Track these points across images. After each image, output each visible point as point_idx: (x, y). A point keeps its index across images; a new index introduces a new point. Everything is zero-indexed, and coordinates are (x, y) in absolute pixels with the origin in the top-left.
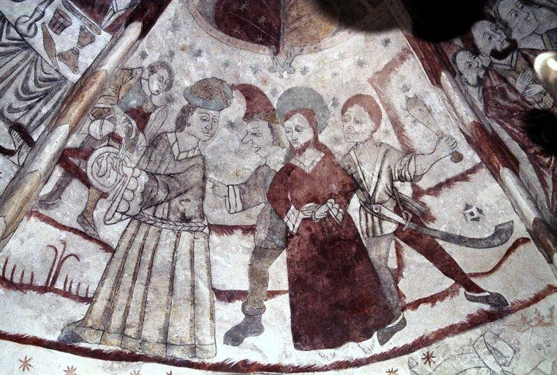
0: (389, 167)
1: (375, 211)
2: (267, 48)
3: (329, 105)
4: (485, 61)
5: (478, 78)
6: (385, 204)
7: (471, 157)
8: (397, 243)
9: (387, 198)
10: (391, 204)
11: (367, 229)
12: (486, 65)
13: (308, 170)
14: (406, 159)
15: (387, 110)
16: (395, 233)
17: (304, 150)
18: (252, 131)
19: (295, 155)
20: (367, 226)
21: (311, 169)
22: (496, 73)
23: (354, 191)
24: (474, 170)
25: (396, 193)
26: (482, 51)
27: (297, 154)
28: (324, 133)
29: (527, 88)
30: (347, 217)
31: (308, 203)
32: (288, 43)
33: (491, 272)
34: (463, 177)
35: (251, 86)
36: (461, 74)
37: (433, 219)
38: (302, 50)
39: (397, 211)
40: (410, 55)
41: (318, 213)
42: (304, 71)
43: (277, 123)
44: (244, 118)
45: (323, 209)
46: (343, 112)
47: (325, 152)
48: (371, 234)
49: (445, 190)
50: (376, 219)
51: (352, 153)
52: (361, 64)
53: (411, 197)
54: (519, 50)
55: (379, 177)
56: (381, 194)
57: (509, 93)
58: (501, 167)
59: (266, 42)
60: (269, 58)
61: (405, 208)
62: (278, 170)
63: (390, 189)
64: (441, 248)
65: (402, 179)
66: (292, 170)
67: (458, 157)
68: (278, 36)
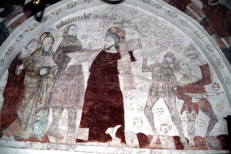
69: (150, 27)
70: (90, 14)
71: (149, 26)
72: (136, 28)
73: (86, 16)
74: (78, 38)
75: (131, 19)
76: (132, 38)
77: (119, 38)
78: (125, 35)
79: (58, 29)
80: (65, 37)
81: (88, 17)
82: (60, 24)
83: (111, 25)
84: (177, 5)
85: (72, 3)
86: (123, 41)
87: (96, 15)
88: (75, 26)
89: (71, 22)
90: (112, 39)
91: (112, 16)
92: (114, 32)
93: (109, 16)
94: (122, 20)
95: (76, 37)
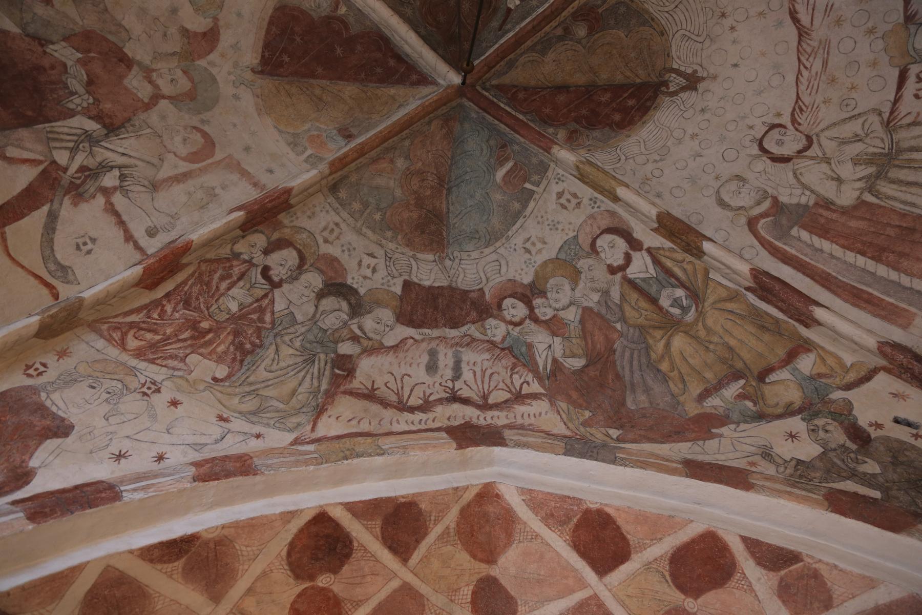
0: (136, 166)
1: (81, 145)
2: (258, 61)
3: (202, 116)
4: (259, 259)
5: (241, 253)
6: (90, 156)
7: (153, 246)
8: (40, 162)
9: (99, 159)
10: (91, 163)
11: (58, 133)
12: (254, 261)
13: (126, 82)
14: (146, 183)
15: (200, 169)
16: (54, 162)
17: (150, 82)
18: (169, 33)
19: (144, 72)
20: (63, 133)
21: (129, 86)
22: (249, 269)
23: (104, 126)
24: (138, 247)
25: (104, 170)
26: (268, 257)
27: (145, 75)
28: (171, 106)
29: (233, 298)
30: (72, 114)
31: (88, 75)
32: (267, 83)
33: (9, 255)
34: (129, 237)
35: (218, 40)
36: (243, 237)
37: (75, 204)
38: (258, 97)
39: (82, 169)
40: (259, 191)
41: (74, 81)
42: (236, 97)
43: (179, 62)
44: (183, 27)
45: (81, 90)
46: (195, 128)
47: (148, 104)
48: (50, 136)
49: (113, 219)
50: (71, 145)
51: (149, 130)
52: (247, 149)
53: (102, 184)
54: (272, 290)
55: (123, 154)
56: (102, 154)
57: (228, 281)
58: (142, 266)
59: (264, 61)
60: (247, 63)
61: (87, 177)
62: (125, 50)
63: (110, 164)
64: (38, 208)
65: (122, 177)
66: (125, 65)
67: (151, 233)
68: (271, 74)
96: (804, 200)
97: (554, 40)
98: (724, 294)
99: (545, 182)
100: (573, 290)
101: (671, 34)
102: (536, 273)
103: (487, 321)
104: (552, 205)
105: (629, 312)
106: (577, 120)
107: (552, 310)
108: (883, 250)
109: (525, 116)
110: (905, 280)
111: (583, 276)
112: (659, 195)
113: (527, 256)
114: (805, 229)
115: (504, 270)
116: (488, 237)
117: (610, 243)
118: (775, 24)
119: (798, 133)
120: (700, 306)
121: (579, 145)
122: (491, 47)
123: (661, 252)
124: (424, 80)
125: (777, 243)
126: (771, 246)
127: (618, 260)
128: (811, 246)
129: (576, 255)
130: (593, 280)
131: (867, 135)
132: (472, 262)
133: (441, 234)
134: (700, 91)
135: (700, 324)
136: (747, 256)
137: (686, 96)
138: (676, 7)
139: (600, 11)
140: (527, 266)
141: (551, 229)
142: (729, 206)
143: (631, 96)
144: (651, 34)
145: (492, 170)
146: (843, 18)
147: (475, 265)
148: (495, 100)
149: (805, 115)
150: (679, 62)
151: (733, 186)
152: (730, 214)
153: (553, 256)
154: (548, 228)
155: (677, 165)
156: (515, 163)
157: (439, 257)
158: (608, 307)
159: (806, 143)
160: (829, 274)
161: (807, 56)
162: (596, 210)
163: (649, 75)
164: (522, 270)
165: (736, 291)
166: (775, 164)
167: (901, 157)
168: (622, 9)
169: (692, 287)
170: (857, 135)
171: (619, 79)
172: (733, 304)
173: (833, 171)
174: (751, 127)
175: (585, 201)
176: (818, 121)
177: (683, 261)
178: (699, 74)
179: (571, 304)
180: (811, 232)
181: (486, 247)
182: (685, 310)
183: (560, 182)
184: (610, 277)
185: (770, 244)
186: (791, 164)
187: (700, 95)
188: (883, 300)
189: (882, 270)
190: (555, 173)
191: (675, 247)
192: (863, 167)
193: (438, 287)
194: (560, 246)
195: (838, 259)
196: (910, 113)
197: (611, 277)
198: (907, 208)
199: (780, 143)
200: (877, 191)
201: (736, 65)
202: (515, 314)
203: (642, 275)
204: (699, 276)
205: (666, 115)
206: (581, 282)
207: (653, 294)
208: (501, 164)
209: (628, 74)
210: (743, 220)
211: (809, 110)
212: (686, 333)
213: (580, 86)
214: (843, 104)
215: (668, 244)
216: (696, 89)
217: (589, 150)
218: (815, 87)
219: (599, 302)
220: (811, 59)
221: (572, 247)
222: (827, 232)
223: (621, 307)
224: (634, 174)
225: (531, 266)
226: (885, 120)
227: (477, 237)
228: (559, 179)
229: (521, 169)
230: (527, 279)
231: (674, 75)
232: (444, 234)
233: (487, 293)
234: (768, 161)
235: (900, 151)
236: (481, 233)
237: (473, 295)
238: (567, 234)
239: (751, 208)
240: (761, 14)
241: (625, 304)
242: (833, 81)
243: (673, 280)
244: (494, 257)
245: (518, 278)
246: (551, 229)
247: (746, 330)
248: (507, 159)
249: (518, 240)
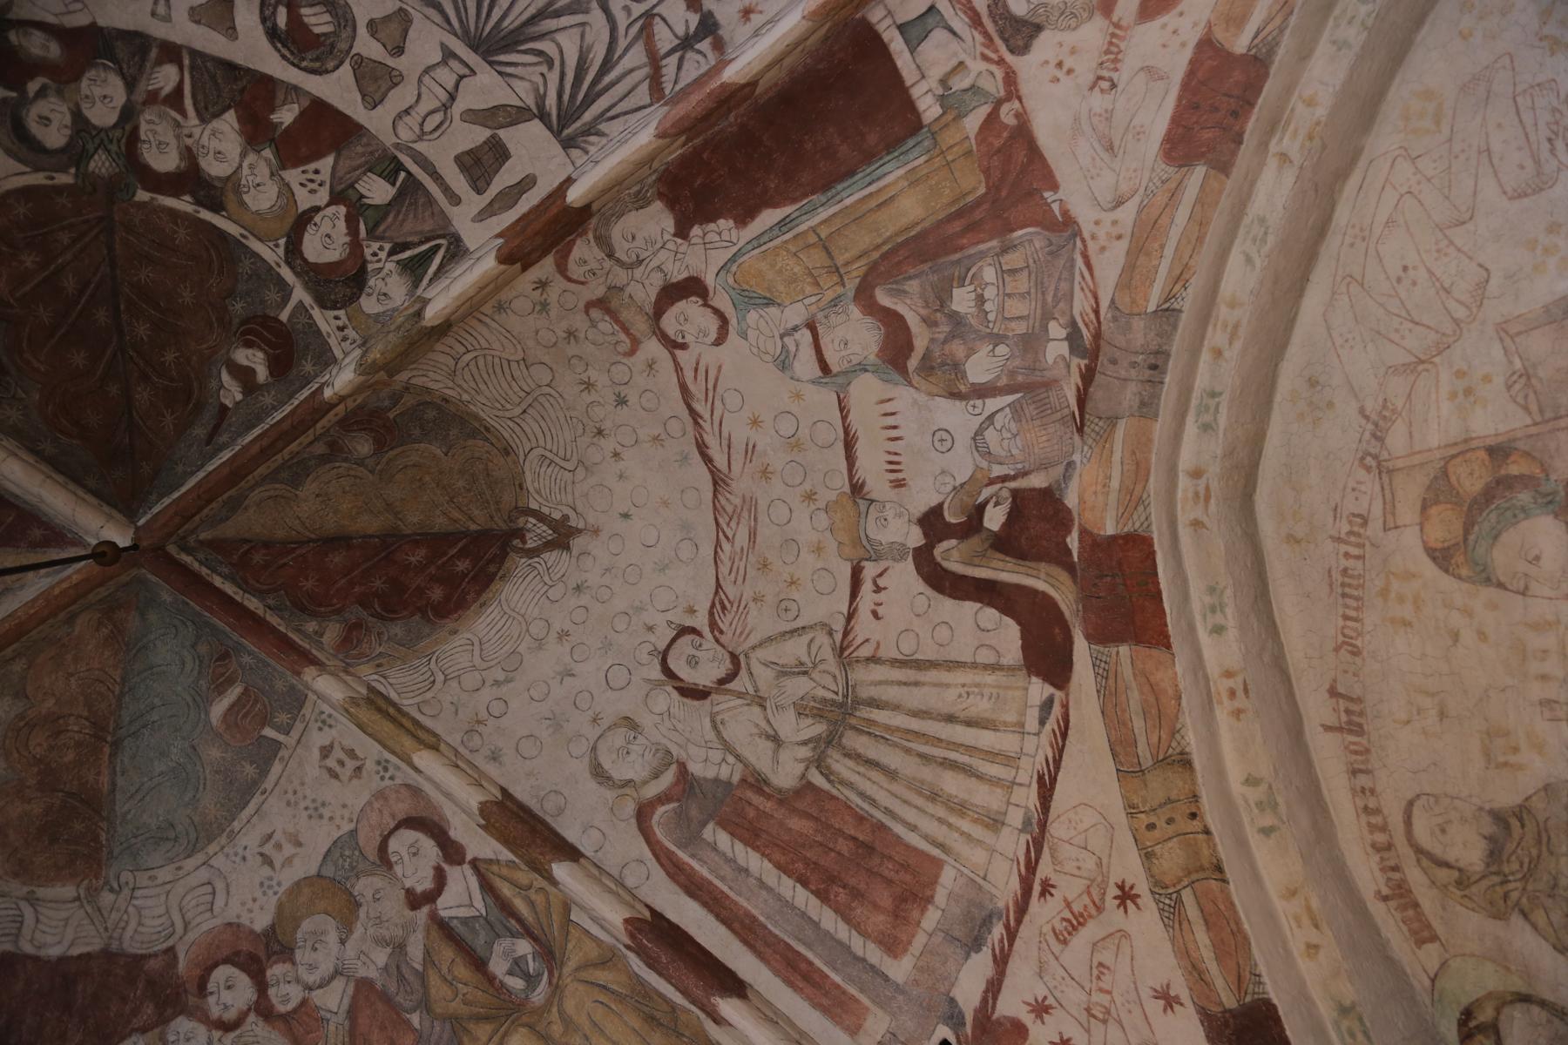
69: (1405, 269)
70: (1333, 693)
71: (1399, 280)
72: (1417, 365)
73: (1344, 718)
74: (1506, 798)
75: (1362, 411)
76: (1499, 381)
77: (1502, 485)
78: (1474, 444)
79: (1434, 938)
80: (1506, 897)
81: (1355, 707)
82: (1398, 915)
83: (1408, 545)
84: (1235, 114)
85: (1253, 805)
86: (1527, 454)
87: (1337, 650)
88: (1411, 804)
89: (1383, 828)
90: (1510, 537)
91: (1339, 540)
92: (1458, 527)
93: (1344, 563)
94: (1368, 469)
95: (1499, 817)
96: (724, 773)
97: (313, 462)
98: (593, 953)
99: (299, 726)
100: (343, 942)
101: (522, 453)
102: (280, 907)
103: (173, 1024)
104: (313, 770)
105: (438, 989)
106: (363, 602)
107: (300, 988)
108: (832, 879)
109: (262, 600)
110: (857, 944)
111: (362, 913)
112: (495, 757)
113: (267, 871)
114: (724, 828)
115: (219, 902)
116: (193, 836)
117: (412, 846)
118: (678, 458)
119: (719, 648)
120: (556, 975)
121: (361, 655)
122: (193, 473)
123: (495, 868)
124: (56, 535)
125: (683, 856)
126: (671, 860)
127: (422, 881)
128: (731, 861)
129: (353, 868)
130: (379, 921)
131: (815, 666)
132: (158, 890)
133: (96, 839)
134: (575, 552)
135: (555, 1010)
136: (630, 882)
137: (553, 558)
138: (525, 411)
139: (391, 415)
140: (264, 894)
141: (310, 817)
142: (609, 778)
143: (461, 554)
144: (487, 452)
145: (202, 703)
146: (770, 469)
147: (163, 898)
148: (204, 571)
149: (729, 617)
150: (540, 500)
151: (619, 738)
152: (610, 795)
153: (313, 871)
154: (305, 814)
155: (532, 691)
156: (246, 689)
157: (88, 889)
158: (401, 978)
159: (731, 666)
160: (754, 919)
161: (727, 519)
162: (387, 782)
163: (492, 518)
164: (254, 900)
165: (612, 950)
166: (685, 700)
167: (858, 714)
168: (431, 414)
169: (543, 938)
170: (802, 664)
171: (440, 523)
172: (606, 973)
173: (768, 721)
174: (650, 629)
175: (370, 765)
176: (746, 632)
177: (530, 887)
178: (573, 523)
179: (337, 973)
180: (732, 834)
181: (189, 856)
182: (531, 980)
183: (326, 729)
184: (409, 913)
185: (670, 855)
186: (707, 702)
187: (574, 560)
188: (827, 977)
189: (829, 920)
190: (317, 711)
191: (517, 861)
192: (810, 721)
193: (80, 957)
194: (325, 850)
195: (770, 890)
196: (867, 640)
197: (412, 913)
198: (866, 806)
199: (693, 662)
200: (828, 768)
201: (626, 516)
202: (230, 1003)
203: (463, 913)
204: (554, 917)
205: (522, 588)
206: (359, 925)
207: (479, 950)
208: (220, 690)
209: (456, 514)
210: (630, 808)
211: (735, 605)
212: (531, 1027)
213: (371, 536)
214: (782, 606)
215: (506, 855)
216: (567, 548)
217: (379, 666)
218: (742, 572)
219: (386, 968)
220: (733, 524)
221: (347, 853)
222: (757, 836)
223: (422, 977)
224: (456, 713)
225: (270, 892)
226: (838, 645)
227: (172, 835)
228: (324, 722)
229: (256, 701)
230: (261, 921)
231: (531, 519)
232: (103, 837)
233: (181, 956)
234: (675, 694)
235: (858, 702)
236: (179, 828)
237: (153, 964)
238: (338, 827)
239: (645, 783)
240: (656, 438)
241: (431, 972)
242: (765, 566)
243: (513, 922)
244: (203, 874)
245: (245, 921)
246: (310, 817)
247: (626, 1023)
248: (230, 682)
249: (250, 840)
